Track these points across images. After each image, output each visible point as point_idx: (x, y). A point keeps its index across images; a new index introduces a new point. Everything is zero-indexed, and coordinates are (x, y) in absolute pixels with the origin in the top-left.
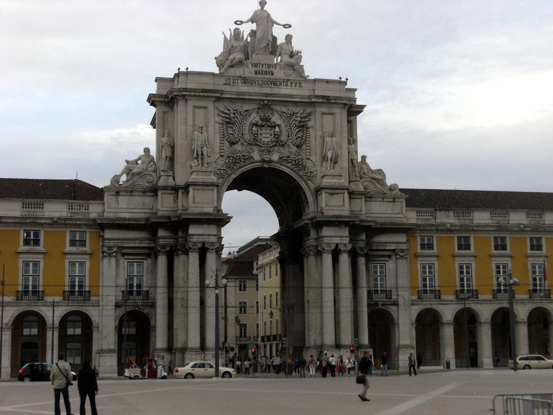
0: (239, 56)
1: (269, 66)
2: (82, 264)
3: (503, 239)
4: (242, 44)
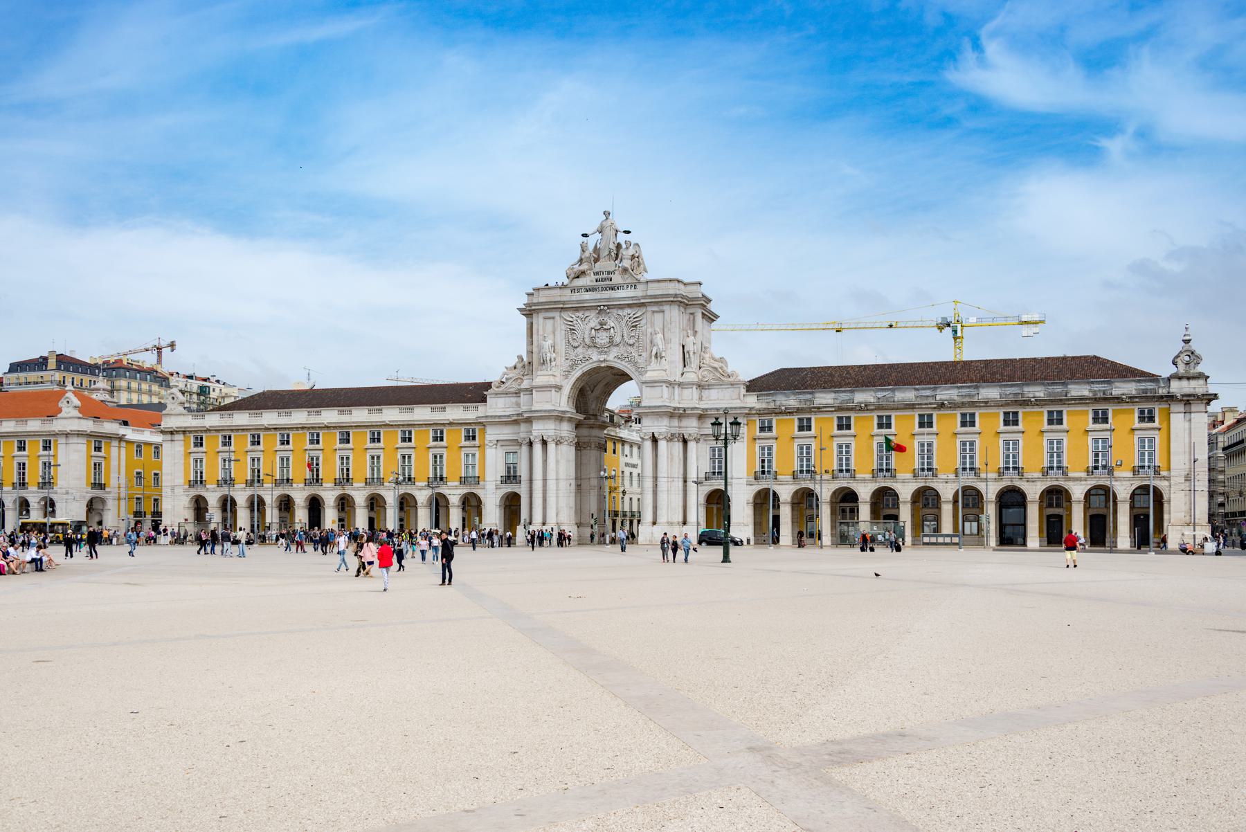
0: (584, 267)
1: (609, 273)
2: (473, 455)
3: (849, 418)
4: (587, 254)
